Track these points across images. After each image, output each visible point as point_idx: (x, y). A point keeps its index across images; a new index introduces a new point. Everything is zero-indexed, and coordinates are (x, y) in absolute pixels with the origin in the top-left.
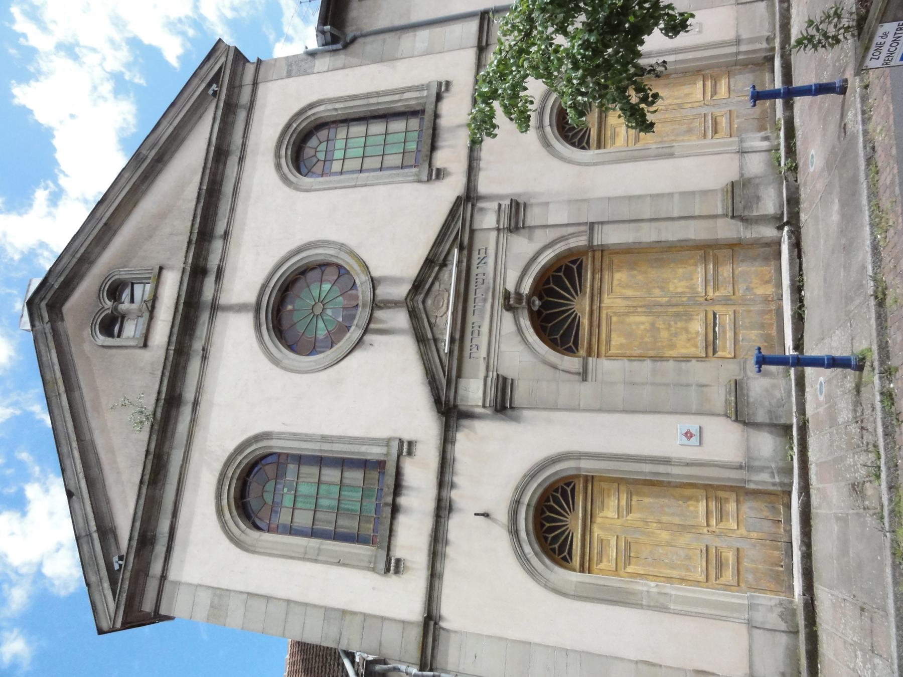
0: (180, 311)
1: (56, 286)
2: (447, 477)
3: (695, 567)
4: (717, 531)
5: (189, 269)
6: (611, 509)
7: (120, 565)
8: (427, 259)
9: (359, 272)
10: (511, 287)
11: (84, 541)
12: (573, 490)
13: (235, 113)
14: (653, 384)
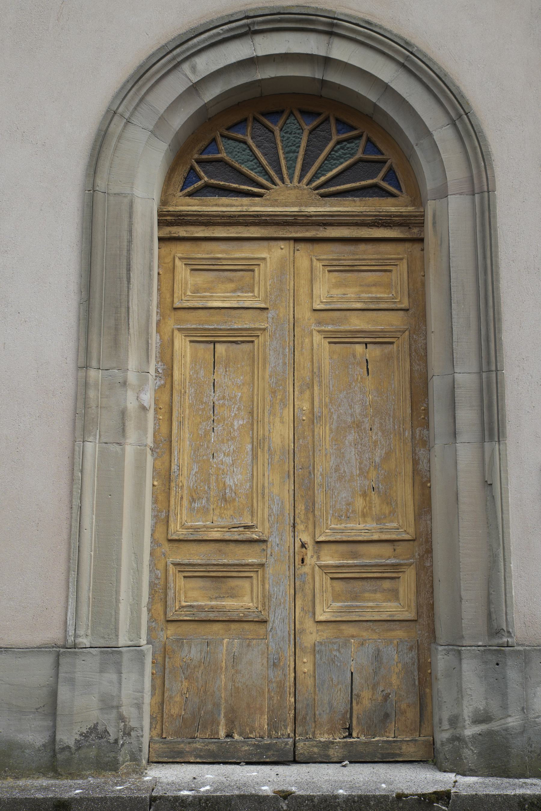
3: (205, 511)
4: (306, 569)
6: (337, 292)
12: (375, 191)
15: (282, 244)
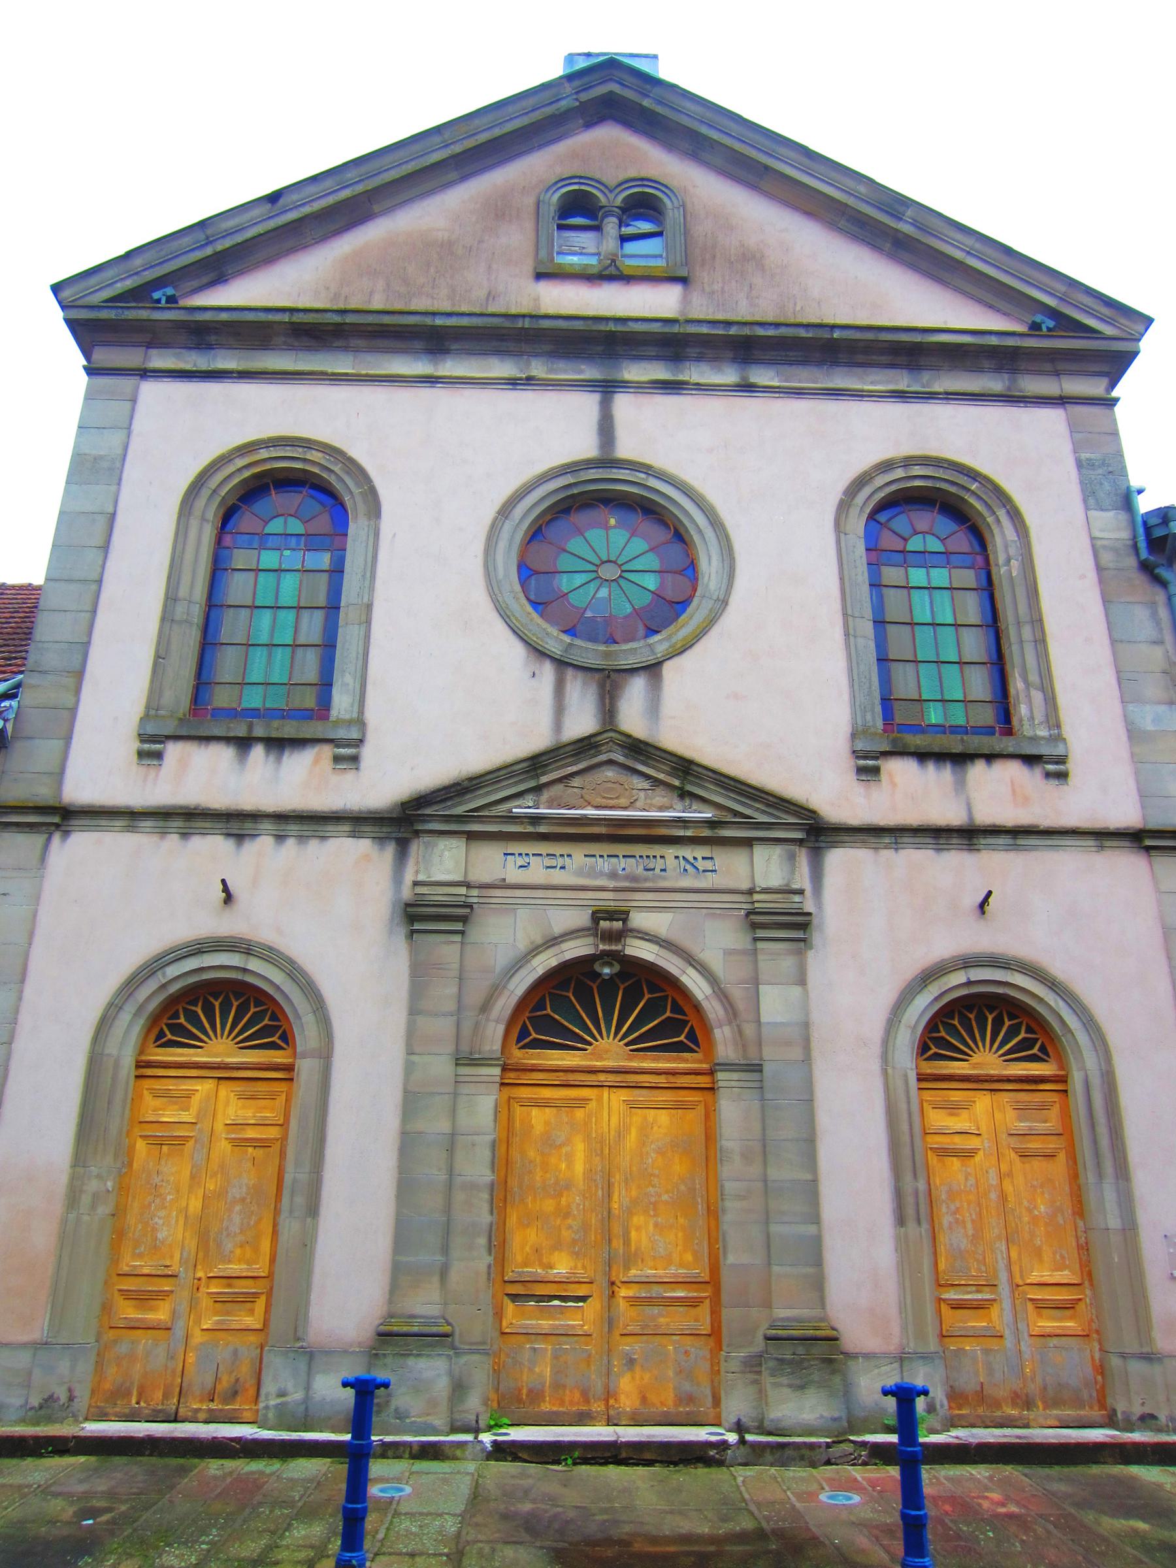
0: (595, 328)
1: (646, 103)
2: (293, 828)
4: (199, 1295)
5: (676, 329)
6: (240, 1112)
7: (159, 301)
8: (691, 762)
9: (674, 640)
10: (639, 920)
11: (200, 236)
13: (999, 369)
14: (449, 1186)
15: (210, 1081)
